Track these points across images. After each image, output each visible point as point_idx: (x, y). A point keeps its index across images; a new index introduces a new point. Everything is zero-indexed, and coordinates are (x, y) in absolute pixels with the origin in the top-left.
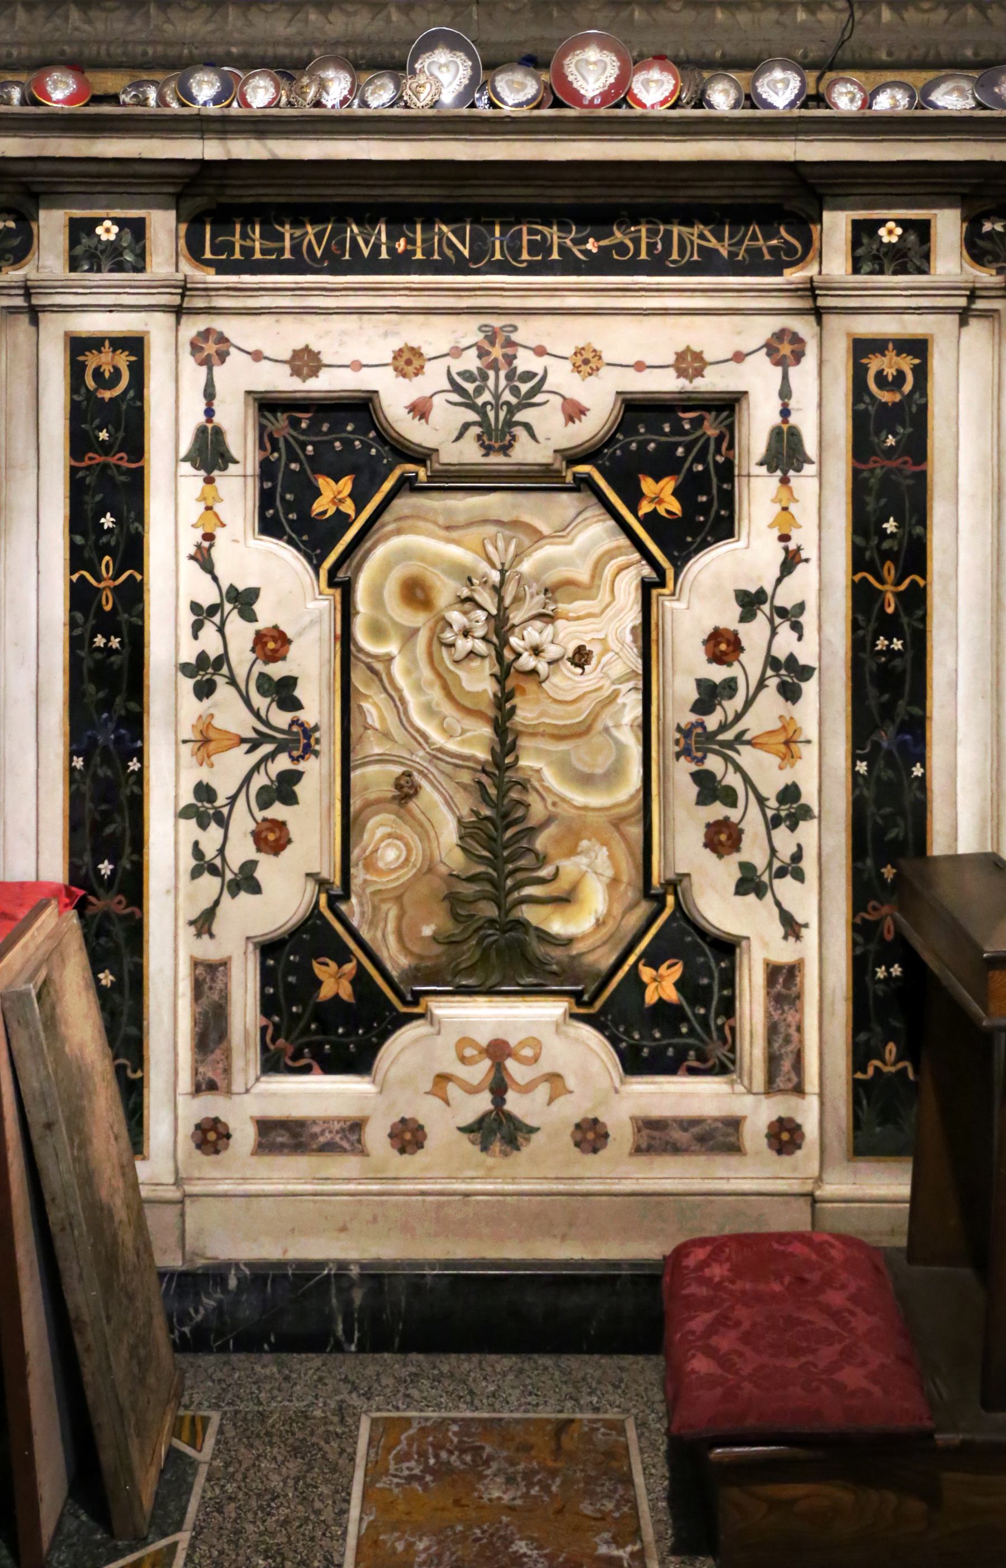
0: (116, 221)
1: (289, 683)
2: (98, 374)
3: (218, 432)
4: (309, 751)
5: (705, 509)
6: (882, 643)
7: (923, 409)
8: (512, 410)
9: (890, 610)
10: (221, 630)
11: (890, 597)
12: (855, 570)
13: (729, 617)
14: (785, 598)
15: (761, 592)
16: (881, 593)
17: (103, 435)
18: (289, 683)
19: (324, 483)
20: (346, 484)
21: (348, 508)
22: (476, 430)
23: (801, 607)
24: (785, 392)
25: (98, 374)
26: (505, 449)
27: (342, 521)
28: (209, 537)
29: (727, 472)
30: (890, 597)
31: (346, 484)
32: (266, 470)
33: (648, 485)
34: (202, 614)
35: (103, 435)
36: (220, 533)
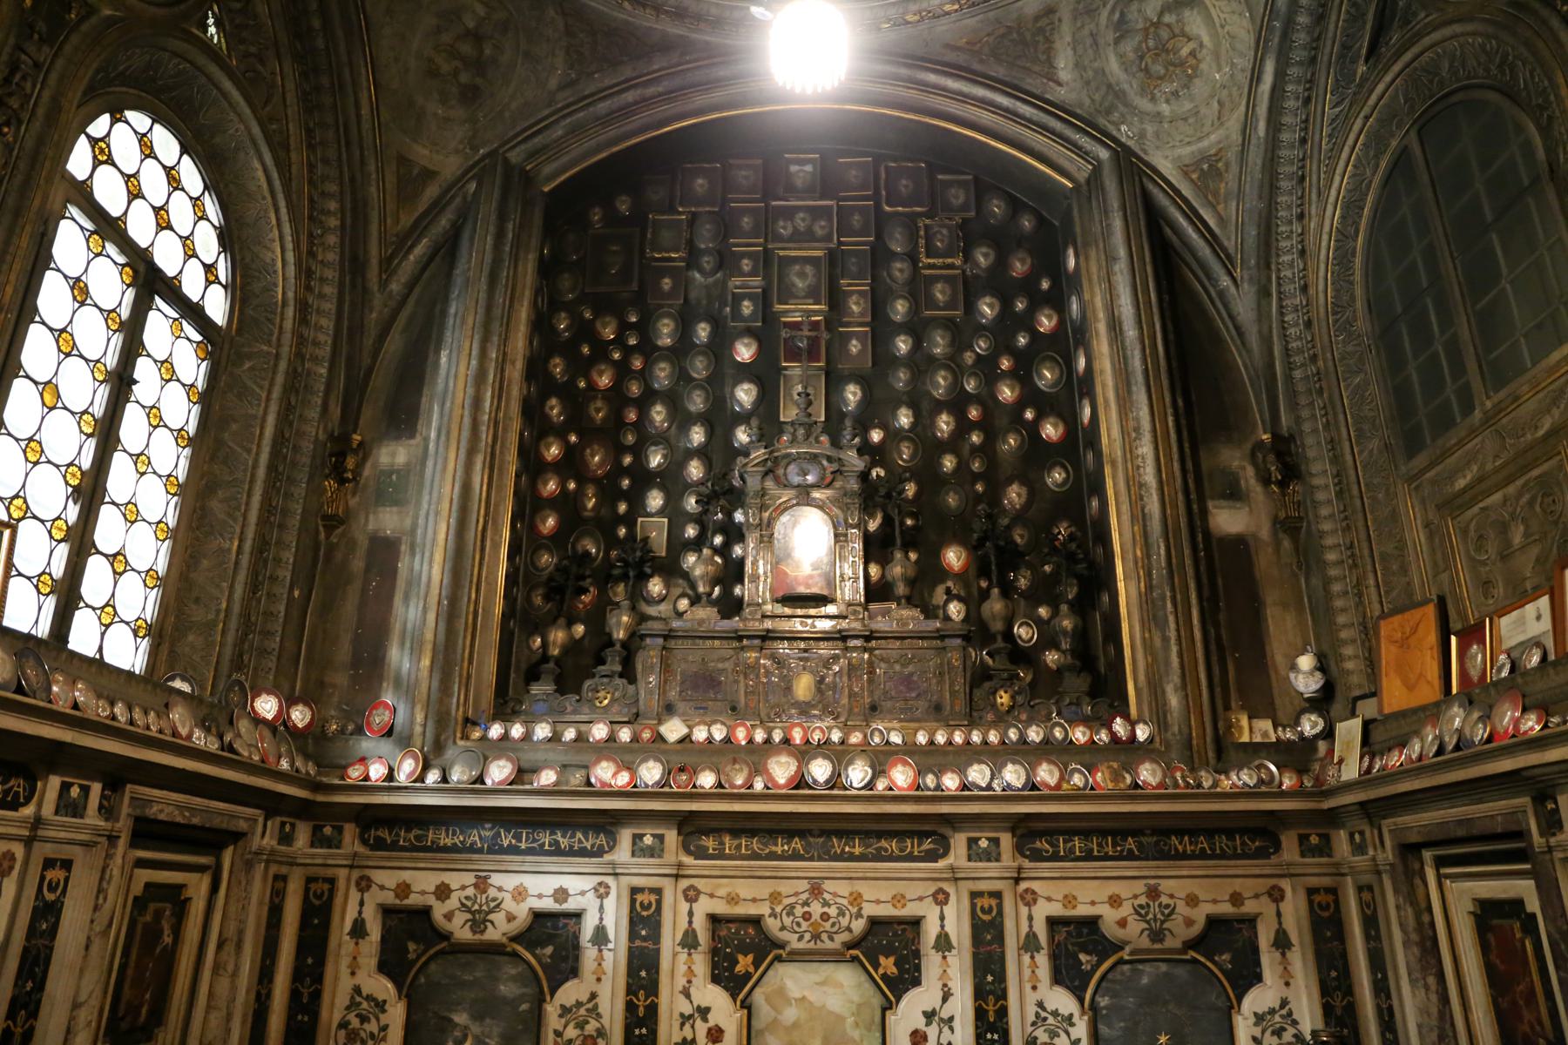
0: (652, 835)
2: (642, 903)
5: (908, 971)
6: (989, 1036)
7: (1002, 924)
9: (992, 1020)
10: (693, 1027)
11: (991, 1013)
12: (976, 1000)
13: (920, 1023)
14: (945, 1014)
15: (934, 1010)
16: (987, 1011)
17: (643, 933)
19: (740, 958)
20: (750, 958)
21: (751, 969)
23: (951, 1019)
24: (942, 918)
25: (642, 903)
27: (748, 976)
28: (689, 982)
29: (917, 954)
30: (991, 1013)
31: (750, 958)
32: (714, 952)
33: (882, 960)
34: (685, 1019)
35: (643, 933)
36: (694, 980)
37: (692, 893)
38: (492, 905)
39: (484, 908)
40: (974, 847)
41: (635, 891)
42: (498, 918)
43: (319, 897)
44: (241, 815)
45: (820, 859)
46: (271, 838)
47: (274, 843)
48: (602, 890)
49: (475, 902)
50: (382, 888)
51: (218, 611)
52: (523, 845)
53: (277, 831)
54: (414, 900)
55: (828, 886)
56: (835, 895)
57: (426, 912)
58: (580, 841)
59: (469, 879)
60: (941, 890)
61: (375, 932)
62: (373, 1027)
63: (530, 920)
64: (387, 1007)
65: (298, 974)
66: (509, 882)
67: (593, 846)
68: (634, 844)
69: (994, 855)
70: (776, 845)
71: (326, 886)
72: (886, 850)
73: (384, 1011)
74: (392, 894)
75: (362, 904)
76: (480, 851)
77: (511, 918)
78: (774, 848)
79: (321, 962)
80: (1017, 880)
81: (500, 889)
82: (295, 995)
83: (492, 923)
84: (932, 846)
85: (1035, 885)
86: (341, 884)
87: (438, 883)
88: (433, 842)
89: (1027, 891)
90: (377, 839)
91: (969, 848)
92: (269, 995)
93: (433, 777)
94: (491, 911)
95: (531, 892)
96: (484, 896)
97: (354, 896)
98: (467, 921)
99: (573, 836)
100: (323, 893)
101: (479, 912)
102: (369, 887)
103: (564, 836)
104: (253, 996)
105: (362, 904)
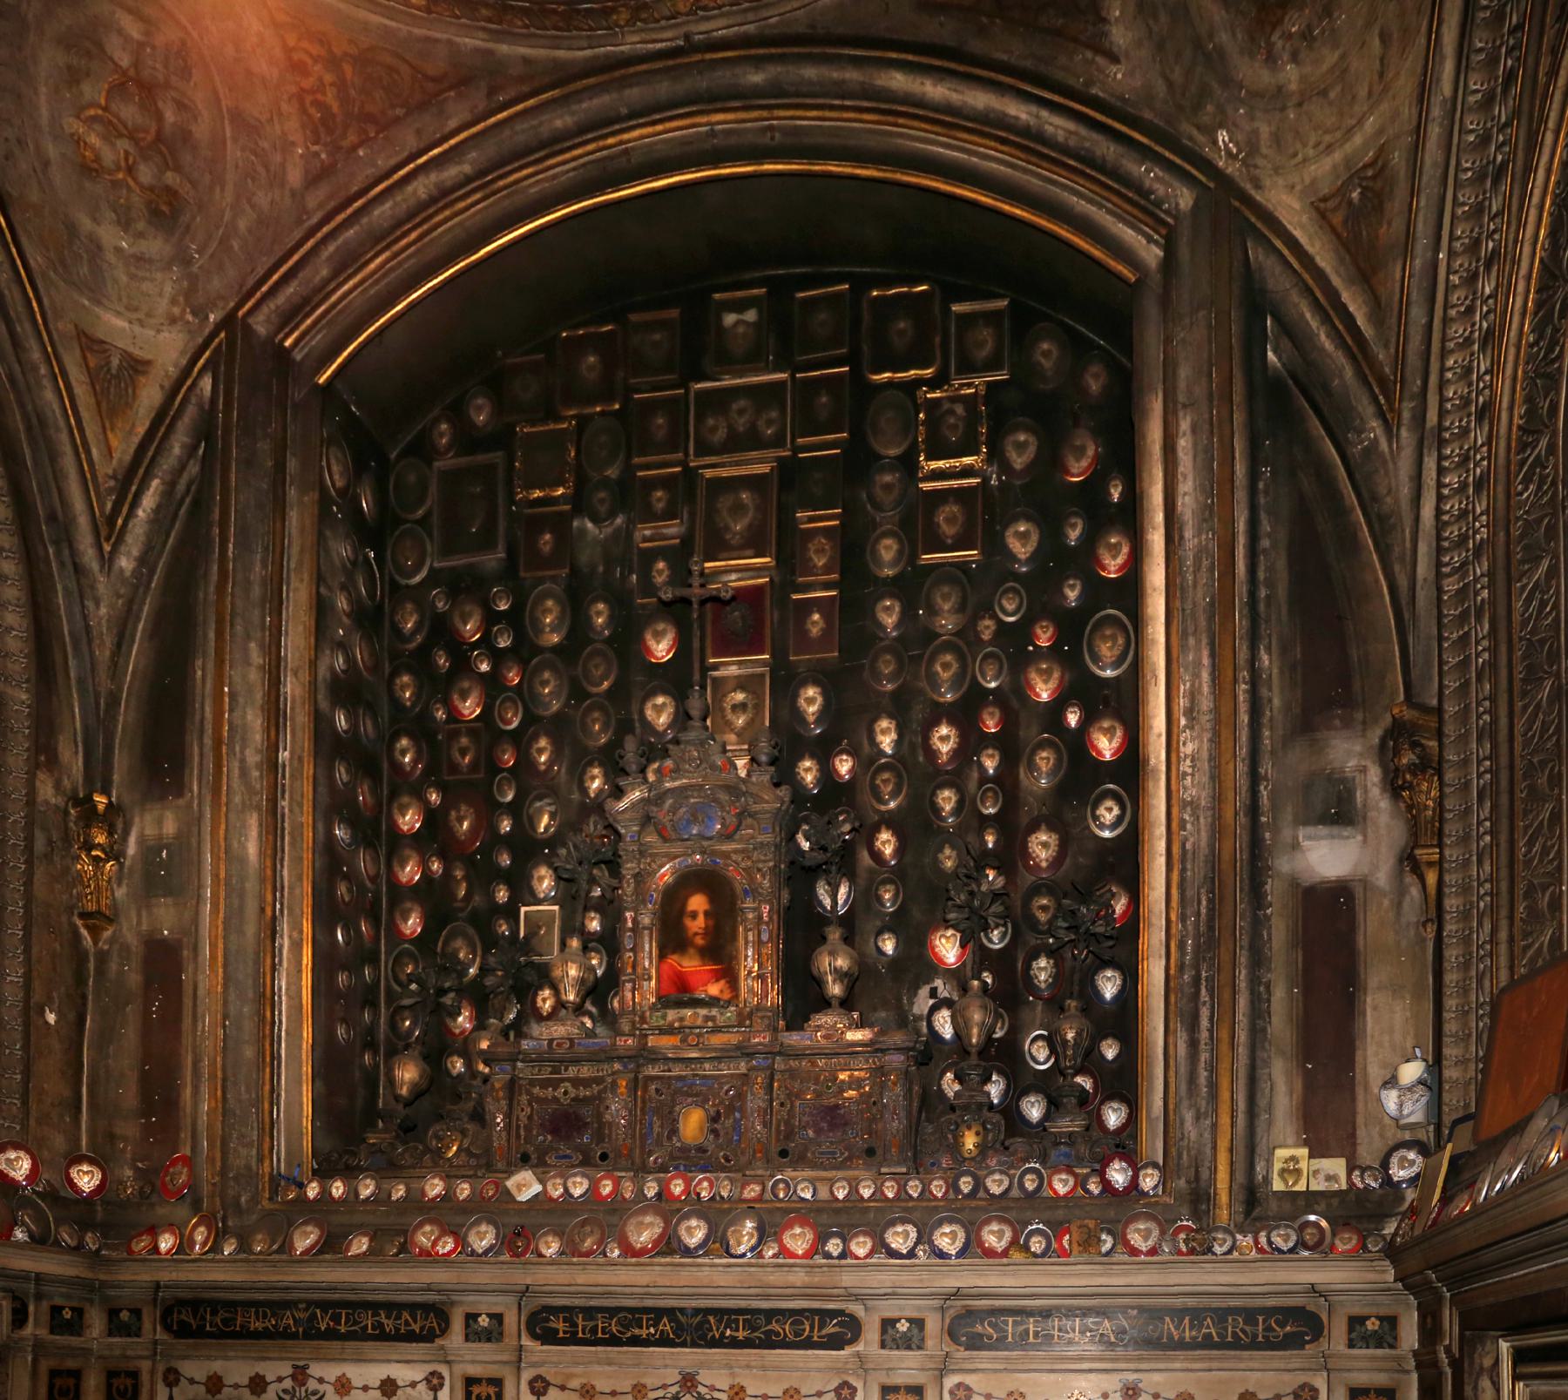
37: (538, 1384)
40: (890, 1331)
41: (470, 1382)
45: (694, 1345)
48: (435, 1381)
52: (343, 1329)
55: (705, 1377)
56: (713, 1388)
58: (407, 1323)
59: (286, 1369)
60: (845, 1384)
67: (422, 1329)
68: (467, 1326)
69: (915, 1340)
70: (641, 1327)
72: (778, 1334)
76: (294, 1336)
78: (637, 1331)
80: (942, 1373)
84: (837, 1329)
85: (969, 1380)
89: (959, 1385)
91: (884, 1331)
99: (398, 1317)
103: (388, 1317)
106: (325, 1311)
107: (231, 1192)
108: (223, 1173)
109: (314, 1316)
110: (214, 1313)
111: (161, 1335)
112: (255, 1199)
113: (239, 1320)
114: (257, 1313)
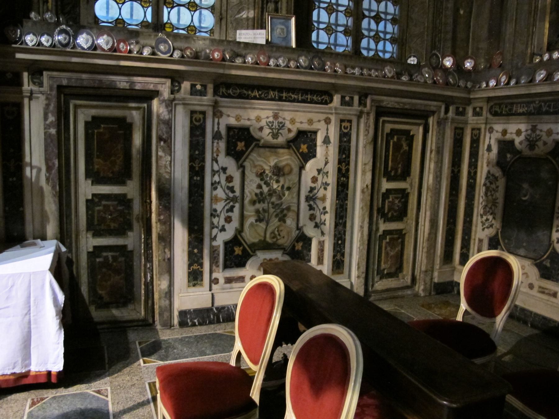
1: (233, 187)
3: (328, 137)
4: (236, 202)
8: (278, 130)
18: (233, 187)
22: (271, 134)
26: (277, 138)
38: (538, 138)
39: (534, 139)
42: (540, 144)
43: (475, 136)
44: (433, 105)
46: (452, 113)
47: (454, 116)
49: (531, 137)
50: (497, 132)
51: (424, 28)
53: (455, 111)
54: (508, 137)
57: (512, 142)
61: (495, 150)
62: (493, 186)
63: (554, 144)
64: (499, 179)
65: (470, 166)
66: (545, 127)
71: (478, 132)
73: (497, 181)
74: (500, 134)
75: (490, 138)
77: (545, 143)
79: (477, 161)
81: (541, 131)
82: (469, 173)
83: (537, 145)
86: (483, 130)
87: (517, 129)
88: (515, 111)
90: (496, 112)
92: (459, 171)
93: (513, 82)
94: (537, 141)
95: (554, 132)
96: (535, 134)
97: (488, 135)
98: (528, 145)
100: (477, 134)
101: (533, 141)
102: (492, 132)
104: (450, 171)
105: (490, 138)
106: (545, 104)
107: (515, 62)
108: (513, 55)
109: (541, 106)
110: (506, 107)
111: (489, 116)
112: (523, 64)
113: (514, 109)
114: (521, 106)
